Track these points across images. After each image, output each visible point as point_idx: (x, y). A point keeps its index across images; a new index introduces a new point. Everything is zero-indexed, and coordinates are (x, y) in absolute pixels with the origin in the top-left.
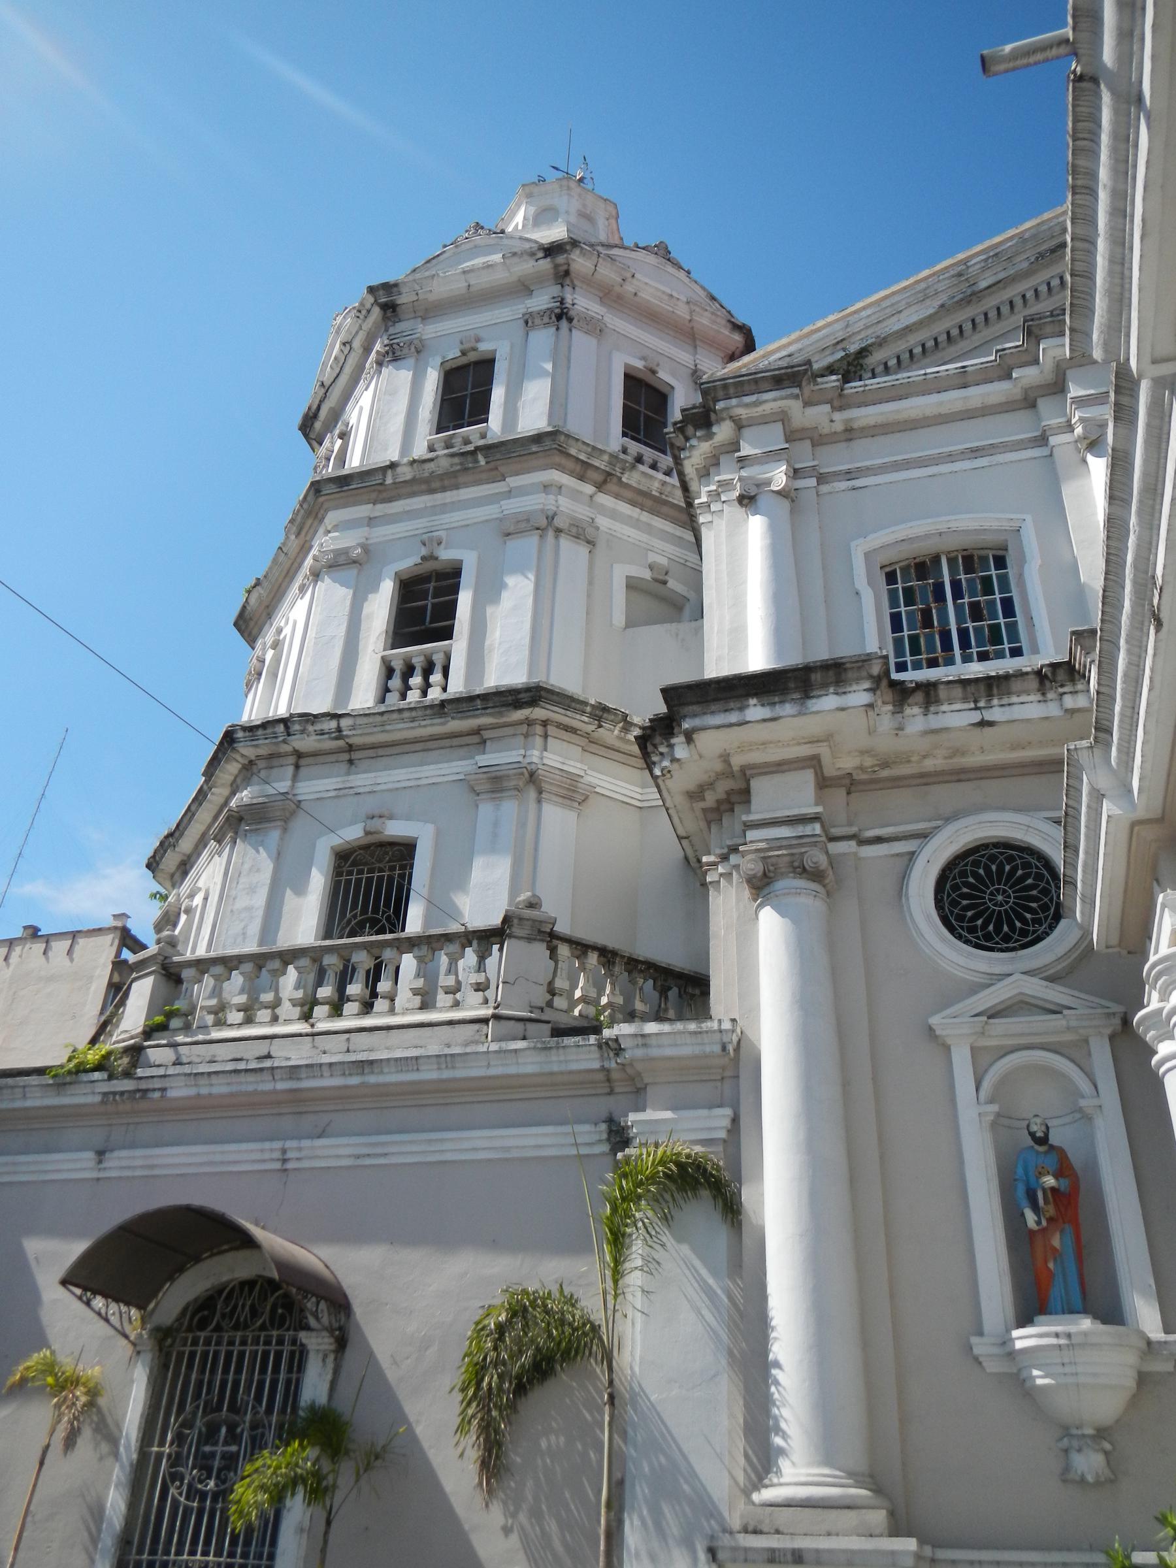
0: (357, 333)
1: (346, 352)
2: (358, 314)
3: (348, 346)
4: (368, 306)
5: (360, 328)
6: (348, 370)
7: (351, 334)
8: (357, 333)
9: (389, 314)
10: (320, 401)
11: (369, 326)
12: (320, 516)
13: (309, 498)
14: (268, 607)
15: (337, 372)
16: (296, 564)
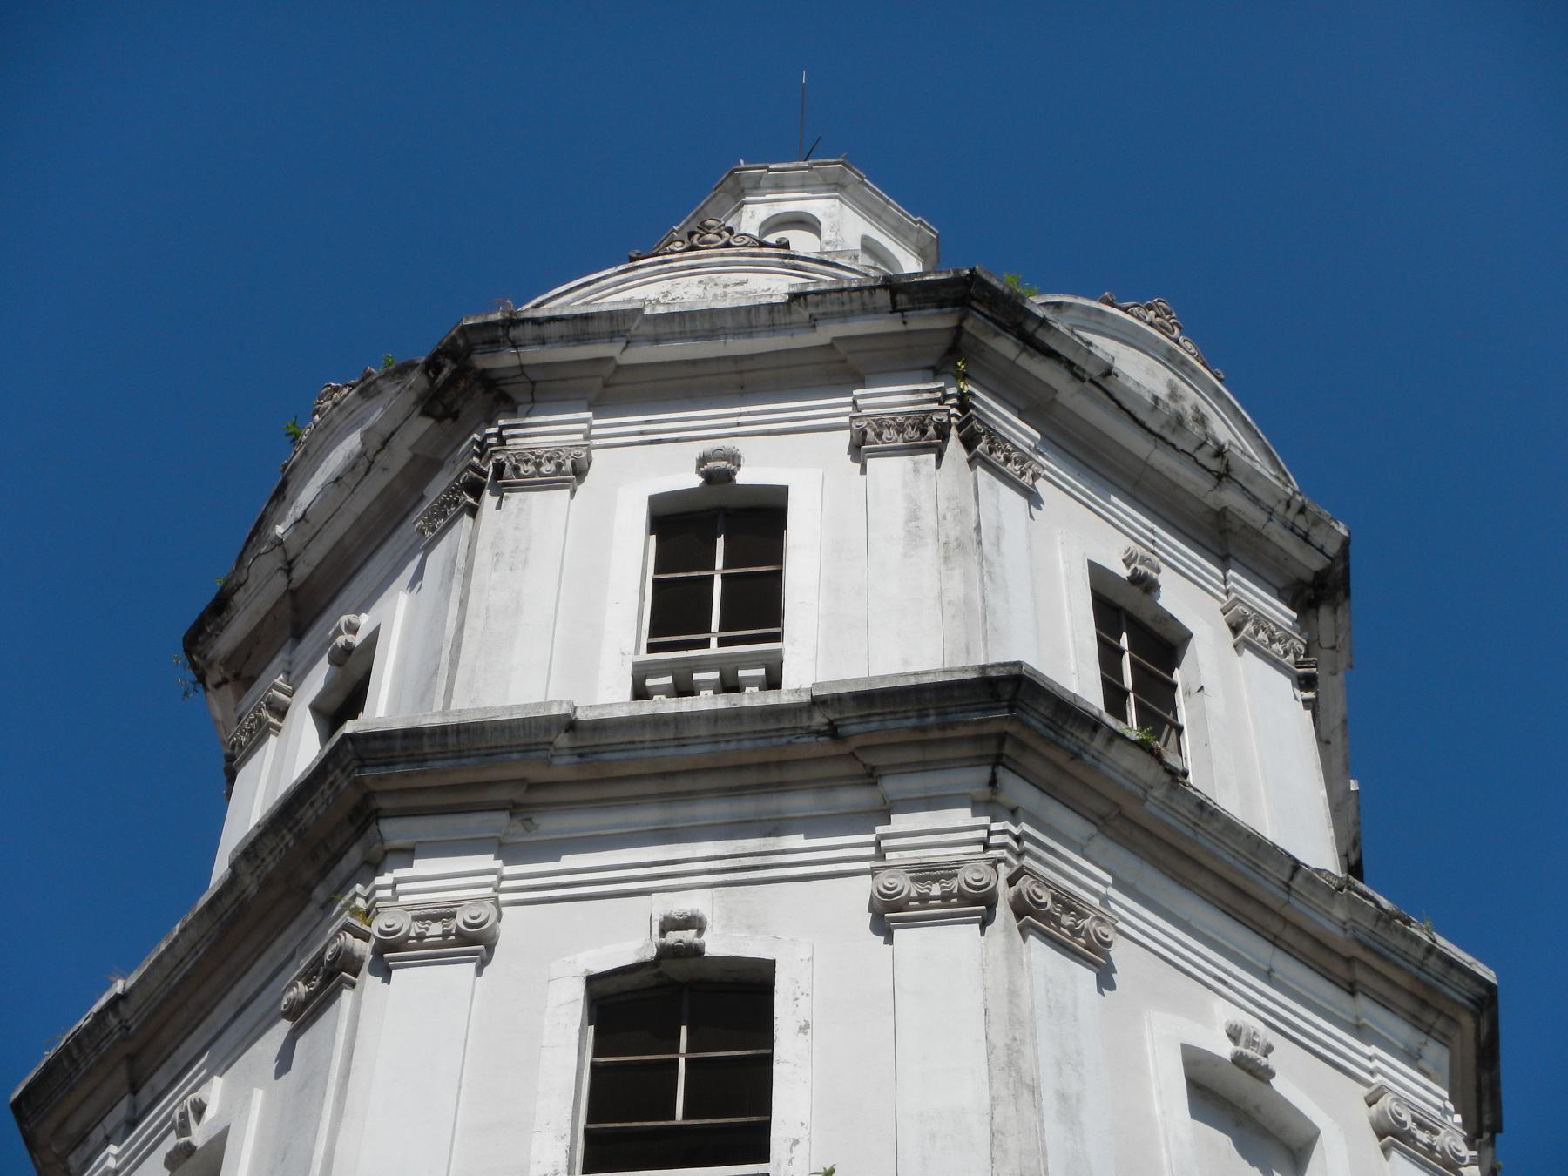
0: (1255, 500)
1: (1203, 457)
2: (1295, 506)
3: (1215, 465)
4: (1318, 537)
5: (1271, 512)
6: (1162, 460)
7: (1247, 479)
8: (1255, 500)
9: (1309, 592)
10: (1070, 365)
11: (1275, 538)
12: (1429, 1018)
13: (1455, 976)
14: (1120, 815)
15: (1149, 424)
16: (1276, 926)
